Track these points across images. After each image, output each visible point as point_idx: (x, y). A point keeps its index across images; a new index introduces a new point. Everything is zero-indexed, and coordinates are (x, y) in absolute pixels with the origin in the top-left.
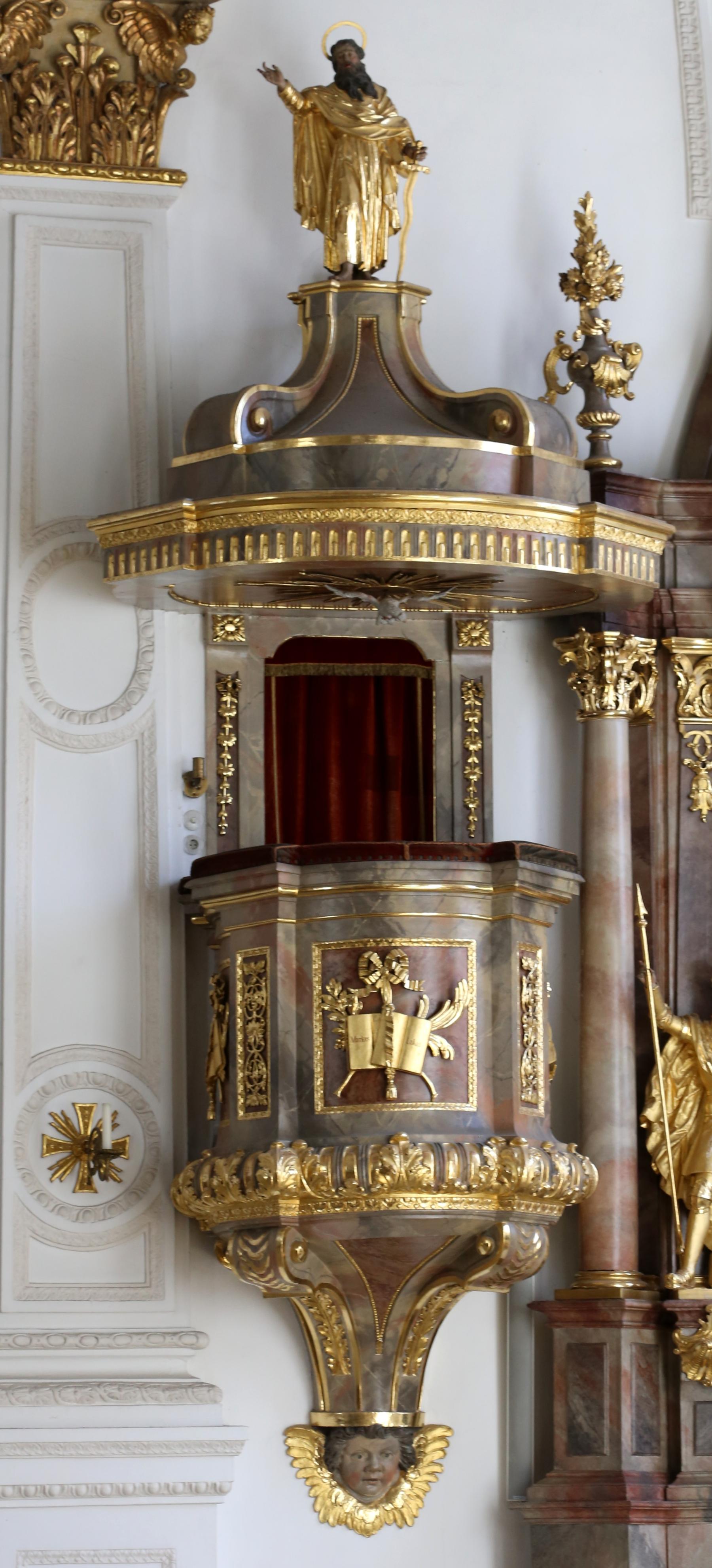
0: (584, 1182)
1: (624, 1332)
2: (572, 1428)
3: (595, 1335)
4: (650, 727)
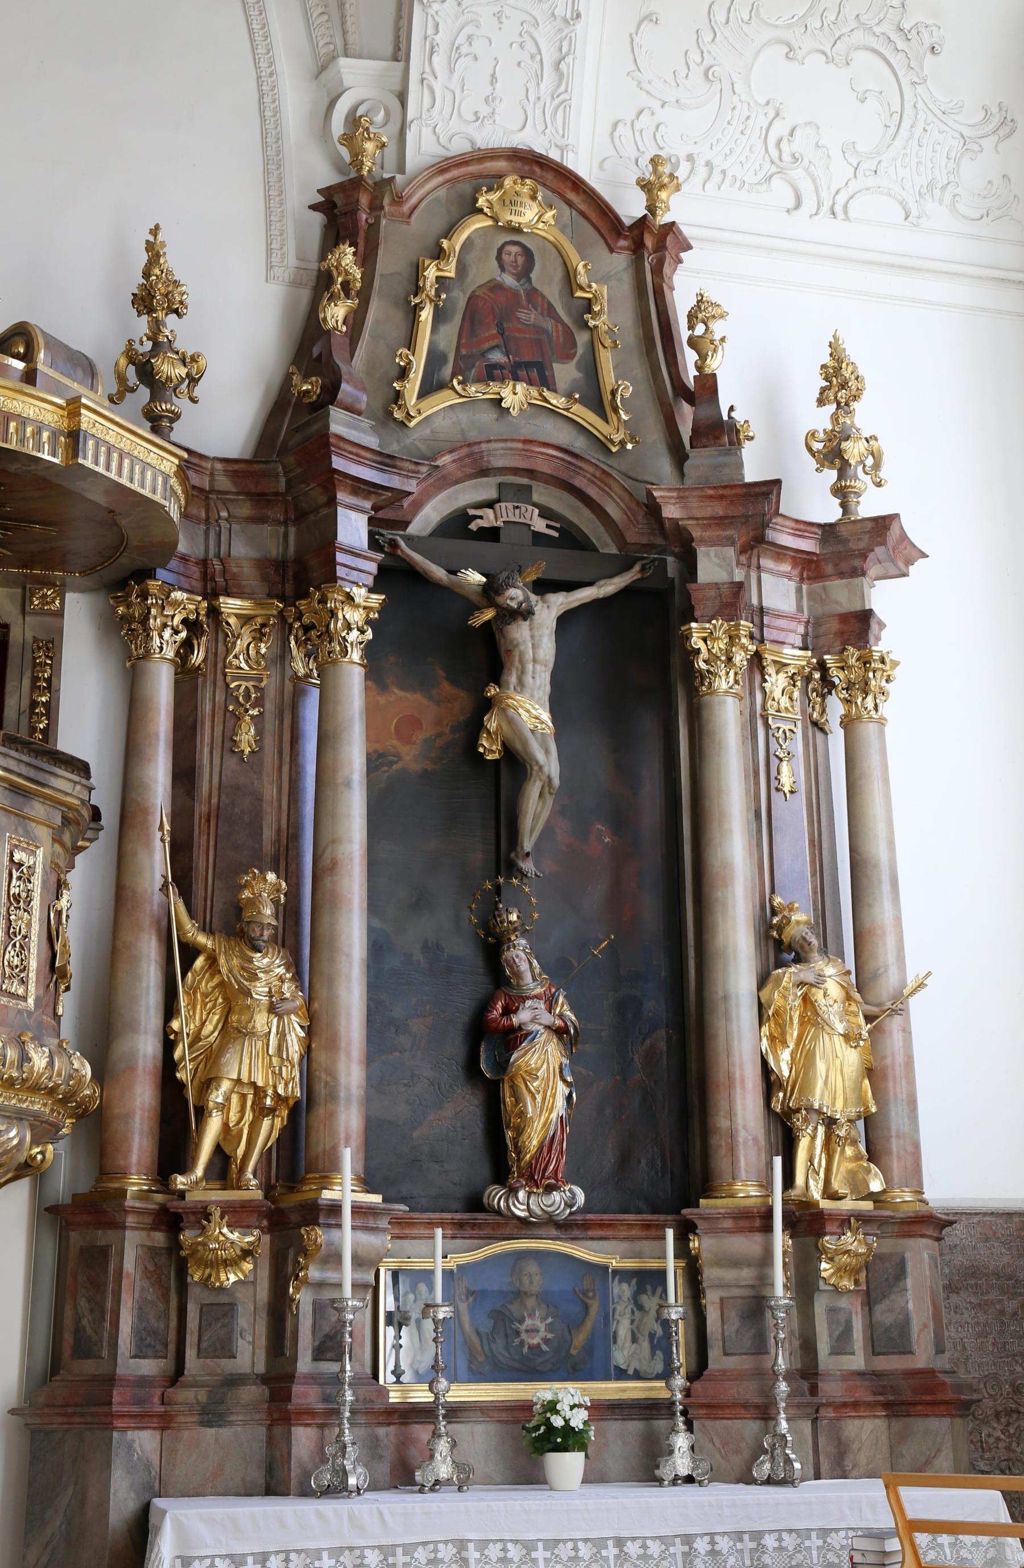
0: (71, 1077)
1: (128, 1233)
2: (78, 1331)
3: (103, 1237)
4: (200, 680)
